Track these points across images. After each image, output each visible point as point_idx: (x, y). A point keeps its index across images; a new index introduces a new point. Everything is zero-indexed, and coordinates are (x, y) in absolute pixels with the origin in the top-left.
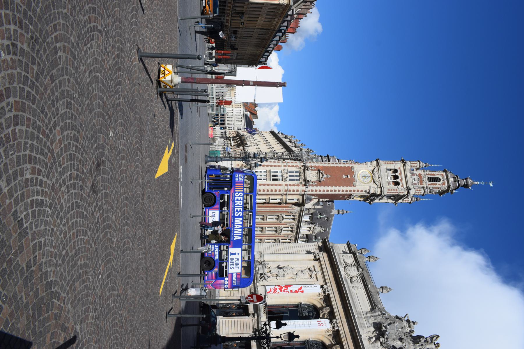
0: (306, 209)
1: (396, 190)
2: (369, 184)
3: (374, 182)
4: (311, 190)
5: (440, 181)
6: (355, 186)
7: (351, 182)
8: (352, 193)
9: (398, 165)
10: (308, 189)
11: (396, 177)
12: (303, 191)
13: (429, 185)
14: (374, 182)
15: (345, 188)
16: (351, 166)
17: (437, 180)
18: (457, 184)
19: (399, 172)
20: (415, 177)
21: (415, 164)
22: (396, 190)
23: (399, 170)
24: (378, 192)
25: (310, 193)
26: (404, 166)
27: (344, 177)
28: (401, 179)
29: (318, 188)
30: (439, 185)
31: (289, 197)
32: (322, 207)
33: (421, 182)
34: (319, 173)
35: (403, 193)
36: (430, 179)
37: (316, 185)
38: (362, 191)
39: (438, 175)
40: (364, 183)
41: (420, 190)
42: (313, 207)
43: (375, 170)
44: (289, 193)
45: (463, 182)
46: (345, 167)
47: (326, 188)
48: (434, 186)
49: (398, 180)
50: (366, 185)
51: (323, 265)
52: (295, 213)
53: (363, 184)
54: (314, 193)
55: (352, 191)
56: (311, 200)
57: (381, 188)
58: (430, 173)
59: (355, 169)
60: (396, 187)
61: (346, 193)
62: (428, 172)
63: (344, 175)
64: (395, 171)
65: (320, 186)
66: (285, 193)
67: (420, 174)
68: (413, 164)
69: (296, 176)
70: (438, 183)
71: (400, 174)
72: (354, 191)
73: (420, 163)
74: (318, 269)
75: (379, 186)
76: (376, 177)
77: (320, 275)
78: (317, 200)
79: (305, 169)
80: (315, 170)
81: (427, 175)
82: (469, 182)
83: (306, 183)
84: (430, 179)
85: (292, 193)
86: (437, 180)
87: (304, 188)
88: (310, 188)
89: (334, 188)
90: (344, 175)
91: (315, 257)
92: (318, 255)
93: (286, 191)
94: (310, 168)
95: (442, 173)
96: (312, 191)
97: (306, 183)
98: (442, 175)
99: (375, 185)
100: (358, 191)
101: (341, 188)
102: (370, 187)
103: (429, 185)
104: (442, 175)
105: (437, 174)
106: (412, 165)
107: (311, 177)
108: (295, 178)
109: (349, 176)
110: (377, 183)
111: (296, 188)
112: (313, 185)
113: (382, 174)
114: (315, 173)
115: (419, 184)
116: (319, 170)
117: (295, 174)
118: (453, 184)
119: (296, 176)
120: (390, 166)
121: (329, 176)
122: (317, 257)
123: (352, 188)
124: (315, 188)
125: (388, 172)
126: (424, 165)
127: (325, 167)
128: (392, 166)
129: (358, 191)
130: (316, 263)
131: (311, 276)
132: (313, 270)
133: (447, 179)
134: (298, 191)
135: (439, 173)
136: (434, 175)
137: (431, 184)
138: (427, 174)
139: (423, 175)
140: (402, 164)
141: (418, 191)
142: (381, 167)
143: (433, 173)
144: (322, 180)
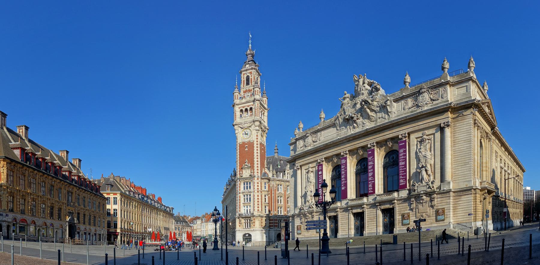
0: (273, 176)
1: (256, 109)
2: (252, 131)
3: (250, 127)
4: (257, 172)
5: (249, 76)
6: (254, 141)
7: (251, 145)
8: (259, 143)
9: (237, 109)
10: (256, 175)
11: (246, 110)
12: (258, 179)
13: (252, 85)
14: (250, 127)
15: (255, 148)
16: (238, 145)
17: (248, 79)
18: (251, 62)
19: (242, 108)
20: (246, 95)
21: (235, 96)
22: (256, 109)
23: (240, 109)
24: (257, 123)
25: (259, 174)
26: (238, 105)
27: (247, 149)
28: (248, 106)
29: (256, 168)
30: (251, 76)
31: (263, 189)
32: (271, 165)
33: (250, 91)
34: (245, 169)
35: (258, 105)
36: (248, 84)
37: (254, 170)
38: (257, 136)
39: (244, 78)
40: (251, 134)
41: (256, 91)
42: (271, 171)
43: (241, 126)
44: (260, 189)
45: (250, 58)
46: (239, 149)
47: (256, 163)
48: (253, 80)
49: (249, 109)
50: (252, 133)
51: (305, 163)
52: (276, 184)
53: (252, 135)
54: (259, 171)
55: (257, 143)
56: (265, 173)
57: (254, 121)
58: (243, 84)
59: (241, 141)
60: (253, 110)
61: (259, 148)
62: (242, 86)
63: (246, 150)
64: (241, 111)
65: (254, 167)
66: (260, 192)
67: (244, 92)
68: (235, 98)
69: (247, 184)
70: (250, 78)
71: (243, 107)
72: (257, 141)
73: (235, 93)
74: (306, 167)
75: (253, 123)
76: (246, 125)
77: (310, 165)
78: (266, 168)
79: (241, 178)
80: (242, 171)
81: (245, 86)
82: (249, 52)
83: (252, 177)
84: (248, 84)
85: (259, 187)
86: (248, 79)
87: (256, 179)
88: (256, 174)
89: (255, 157)
90: (246, 150)
91: (298, 169)
92: (298, 166)
93: (258, 192)
94: (241, 175)
95: (242, 75)
96: (258, 172)
97: (252, 177)
98: (244, 74)
99: (253, 126)
100: (257, 139)
101: (255, 151)
102: (254, 130)
103: (252, 85)
104: (244, 74)
105: (244, 78)
106: (236, 99)
107: (247, 173)
108: (249, 185)
109: (246, 146)
110: (251, 124)
111: (256, 185)
112: (254, 172)
113: (244, 121)
114: (244, 171)
115: (251, 92)
116: (242, 168)
117: (246, 185)
118: (251, 66)
119: (247, 184)
120: (237, 115)
121: (247, 160)
122: (299, 167)
123: (255, 143)
124: (256, 171)
125: (242, 116)
126: (236, 89)
127: (239, 164)
128: (238, 113)
129: (257, 139)
130: (303, 168)
131: (312, 172)
132: (307, 170)
133: (247, 70)
134: (258, 183)
135: (243, 77)
136: (244, 81)
137: (251, 83)
138: (244, 87)
139: (245, 90)
140: (236, 106)
141: (257, 92)
142: (238, 122)
143: (243, 82)
144: (249, 166)
